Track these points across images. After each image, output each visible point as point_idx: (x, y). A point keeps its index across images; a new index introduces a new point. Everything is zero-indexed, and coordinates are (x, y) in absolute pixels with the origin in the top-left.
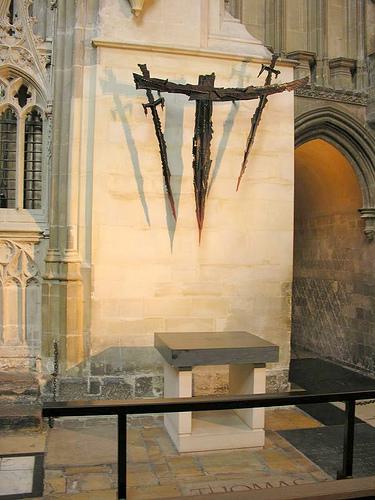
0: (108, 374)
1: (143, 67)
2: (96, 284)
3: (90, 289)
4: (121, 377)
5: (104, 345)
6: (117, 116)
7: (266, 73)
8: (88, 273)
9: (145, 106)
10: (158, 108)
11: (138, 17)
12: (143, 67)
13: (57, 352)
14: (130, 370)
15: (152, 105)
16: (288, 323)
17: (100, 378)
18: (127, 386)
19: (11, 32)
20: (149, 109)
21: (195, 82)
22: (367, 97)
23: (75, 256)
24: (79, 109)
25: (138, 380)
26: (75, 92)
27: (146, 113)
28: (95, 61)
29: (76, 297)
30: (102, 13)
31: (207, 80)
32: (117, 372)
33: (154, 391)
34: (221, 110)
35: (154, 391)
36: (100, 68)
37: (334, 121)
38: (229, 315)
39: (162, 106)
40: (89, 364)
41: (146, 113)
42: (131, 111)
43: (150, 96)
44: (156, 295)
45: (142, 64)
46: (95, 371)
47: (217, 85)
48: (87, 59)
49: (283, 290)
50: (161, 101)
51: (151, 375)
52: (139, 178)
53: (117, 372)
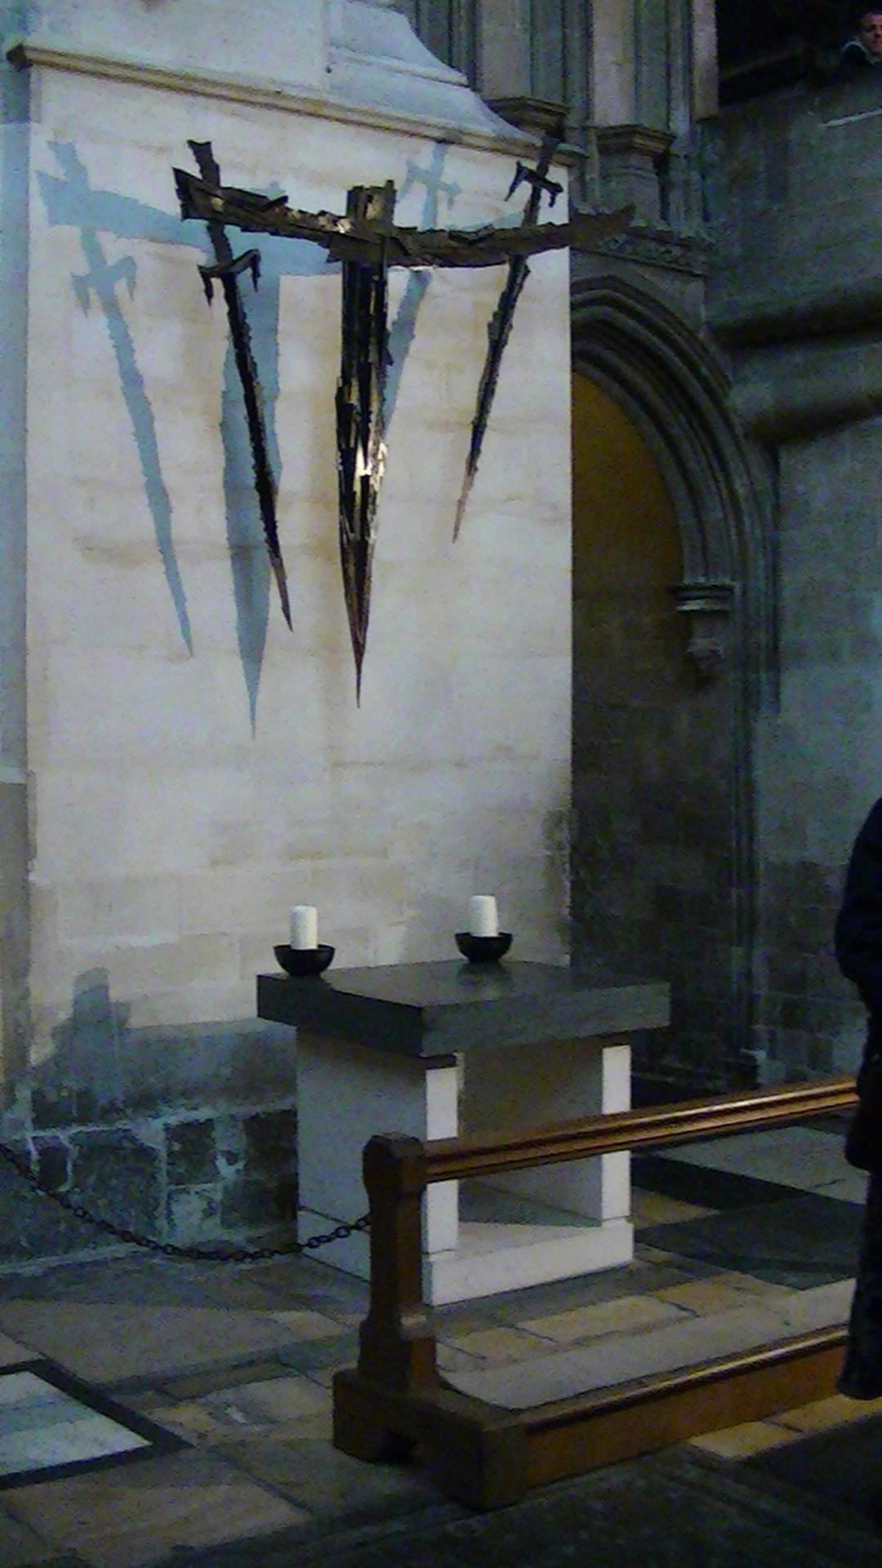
0: (82, 1121)
1: (202, 151)
4: (122, 1124)
6: (92, 291)
7: (526, 189)
9: (206, 274)
12: (202, 151)
14: (146, 1102)
17: (63, 1136)
18: (145, 1153)
20: (217, 284)
22: (709, 248)
25: (171, 1132)
27: (209, 293)
32: (111, 1111)
33: (221, 1163)
35: (221, 1163)
37: (622, 319)
38: (411, 912)
39: (256, 275)
40: (24, 1093)
41: (209, 293)
42: (132, 286)
43: (220, 244)
44: (215, 863)
45: (201, 141)
46: (44, 1114)
49: (549, 834)
50: (253, 259)
51: (203, 1114)
52: (159, 496)
53: (111, 1111)
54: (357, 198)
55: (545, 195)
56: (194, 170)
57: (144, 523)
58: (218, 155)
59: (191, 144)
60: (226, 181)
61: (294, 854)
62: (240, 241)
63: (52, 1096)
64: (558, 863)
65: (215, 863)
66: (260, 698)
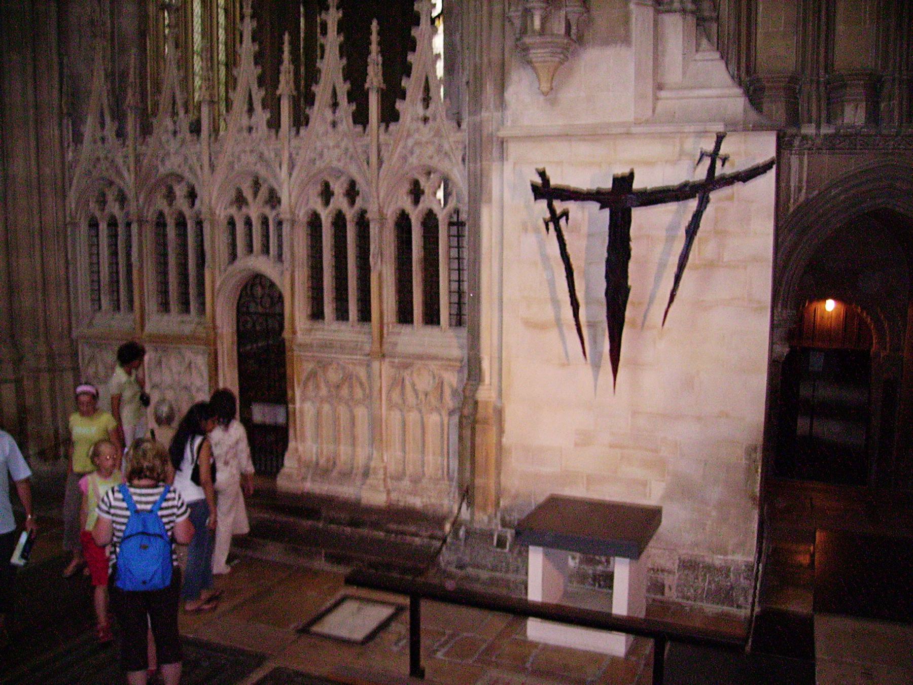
1: (542, 174)
2: (507, 426)
3: (501, 431)
5: (516, 497)
7: (707, 162)
8: (499, 412)
10: (562, 222)
11: (550, 95)
12: (542, 174)
13: (467, 493)
15: (555, 218)
16: (753, 499)
19: (425, 120)
20: (551, 226)
21: (608, 185)
23: (486, 393)
24: (488, 217)
26: (485, 197)
27: (548, 229)
28: (502, 158)
29: (487, 439)
30: (509, 95)
31: (623, 182)
34: (640, 216)
36: (508, 167)
39: (567, 219)
40: (499, 515)
41: (548, 229)
45: (540, 167)
47: (637, 185)
48: (496, 153)
50: (565, 214)
54: (616, 180)
55: (719, 163)
56: (538, 180)
57: (548, 313)
58: (548, 173)
59: (537, 170)
60: (553, 182)
61: (612, 446)
62: (559, 206)
63: (508, 518)
64: (753, 468)
65: (576, 445)
66: (599, 383)
